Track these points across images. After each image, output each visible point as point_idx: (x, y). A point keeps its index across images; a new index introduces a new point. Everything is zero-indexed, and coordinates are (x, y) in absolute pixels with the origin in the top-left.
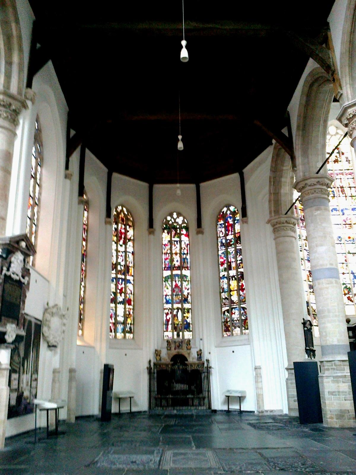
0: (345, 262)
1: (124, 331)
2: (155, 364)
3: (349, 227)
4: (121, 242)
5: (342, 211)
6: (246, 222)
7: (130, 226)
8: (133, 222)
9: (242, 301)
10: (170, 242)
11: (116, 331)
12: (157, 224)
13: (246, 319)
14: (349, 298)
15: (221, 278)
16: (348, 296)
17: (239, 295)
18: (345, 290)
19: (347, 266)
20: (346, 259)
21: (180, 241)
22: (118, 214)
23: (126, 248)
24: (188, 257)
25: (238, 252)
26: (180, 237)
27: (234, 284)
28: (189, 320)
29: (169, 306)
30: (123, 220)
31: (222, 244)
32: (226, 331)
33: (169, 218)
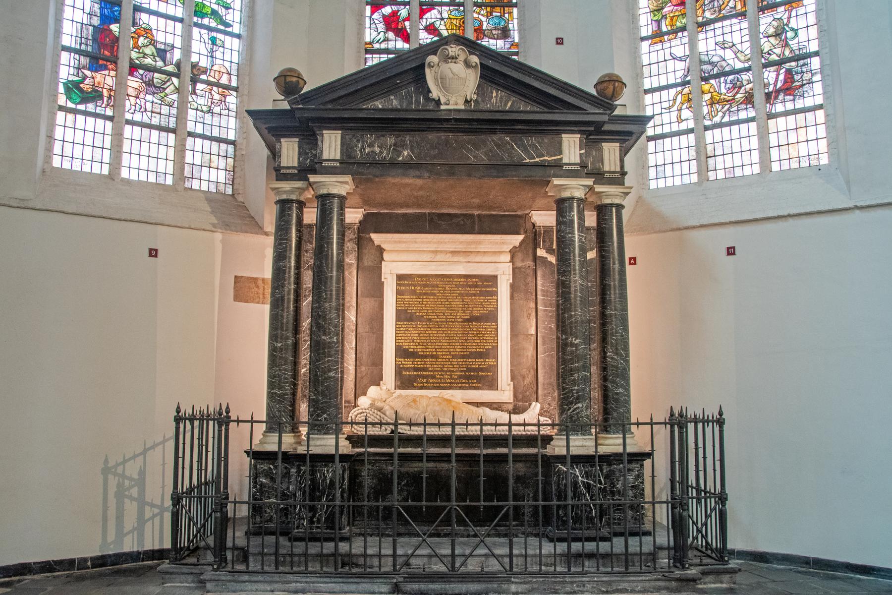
16: (387, 10)
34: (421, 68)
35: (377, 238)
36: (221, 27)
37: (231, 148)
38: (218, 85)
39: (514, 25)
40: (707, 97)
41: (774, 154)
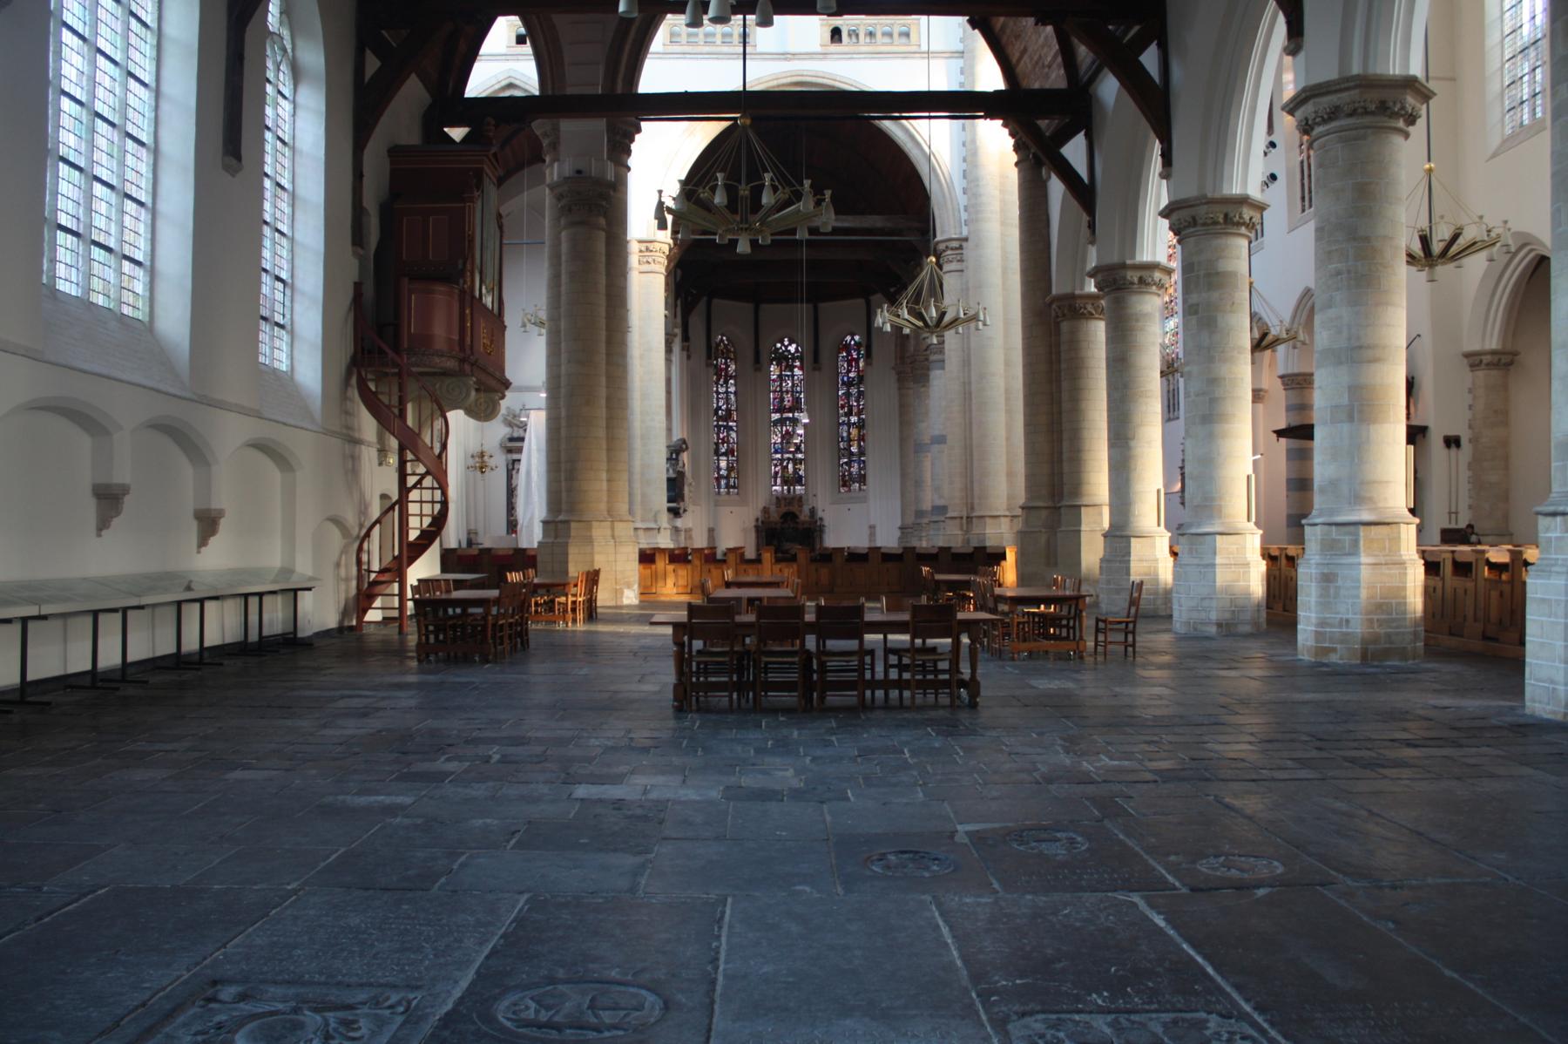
1: (728, 486)
2: (763, 522)
4: (721, 382)
6: (871, 364)
7: (731, 359)
8: (734, 353)
9: (862, 452)
10: (780, 376)
11: (719, 487)
12: (764, 357)
13: (865, 475)
15: (840, 424)
17: (859, 446)
21: (793, 376)
22: (718, 345)
23: (727, 388)
24: (802, 396)
25: (860, 394)
26: (793, 371)
27: (854, 432)
28: (800, 473)
29: (779, 456)
30: (723, 353)
31: (844, 383)
32: (844, 485)
33: (779, 345)
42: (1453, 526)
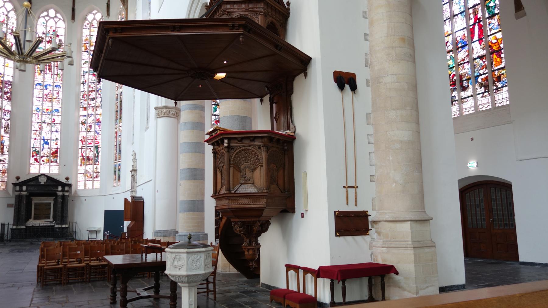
0: (38, 129)
3: (49, 101)
5: (46, 86)
14: (36, 160)
16: (35, 157)
18: (34, 152)
19: (40, 133)
20: (40, 127)
34: (38, 178)
35: (32, 198)
36: (4, 163)
37: (6, 183)
38: (3, 173)
39: (58, 161)
40: (87, 176)
41: (94, 186)
42: (352, 208)
